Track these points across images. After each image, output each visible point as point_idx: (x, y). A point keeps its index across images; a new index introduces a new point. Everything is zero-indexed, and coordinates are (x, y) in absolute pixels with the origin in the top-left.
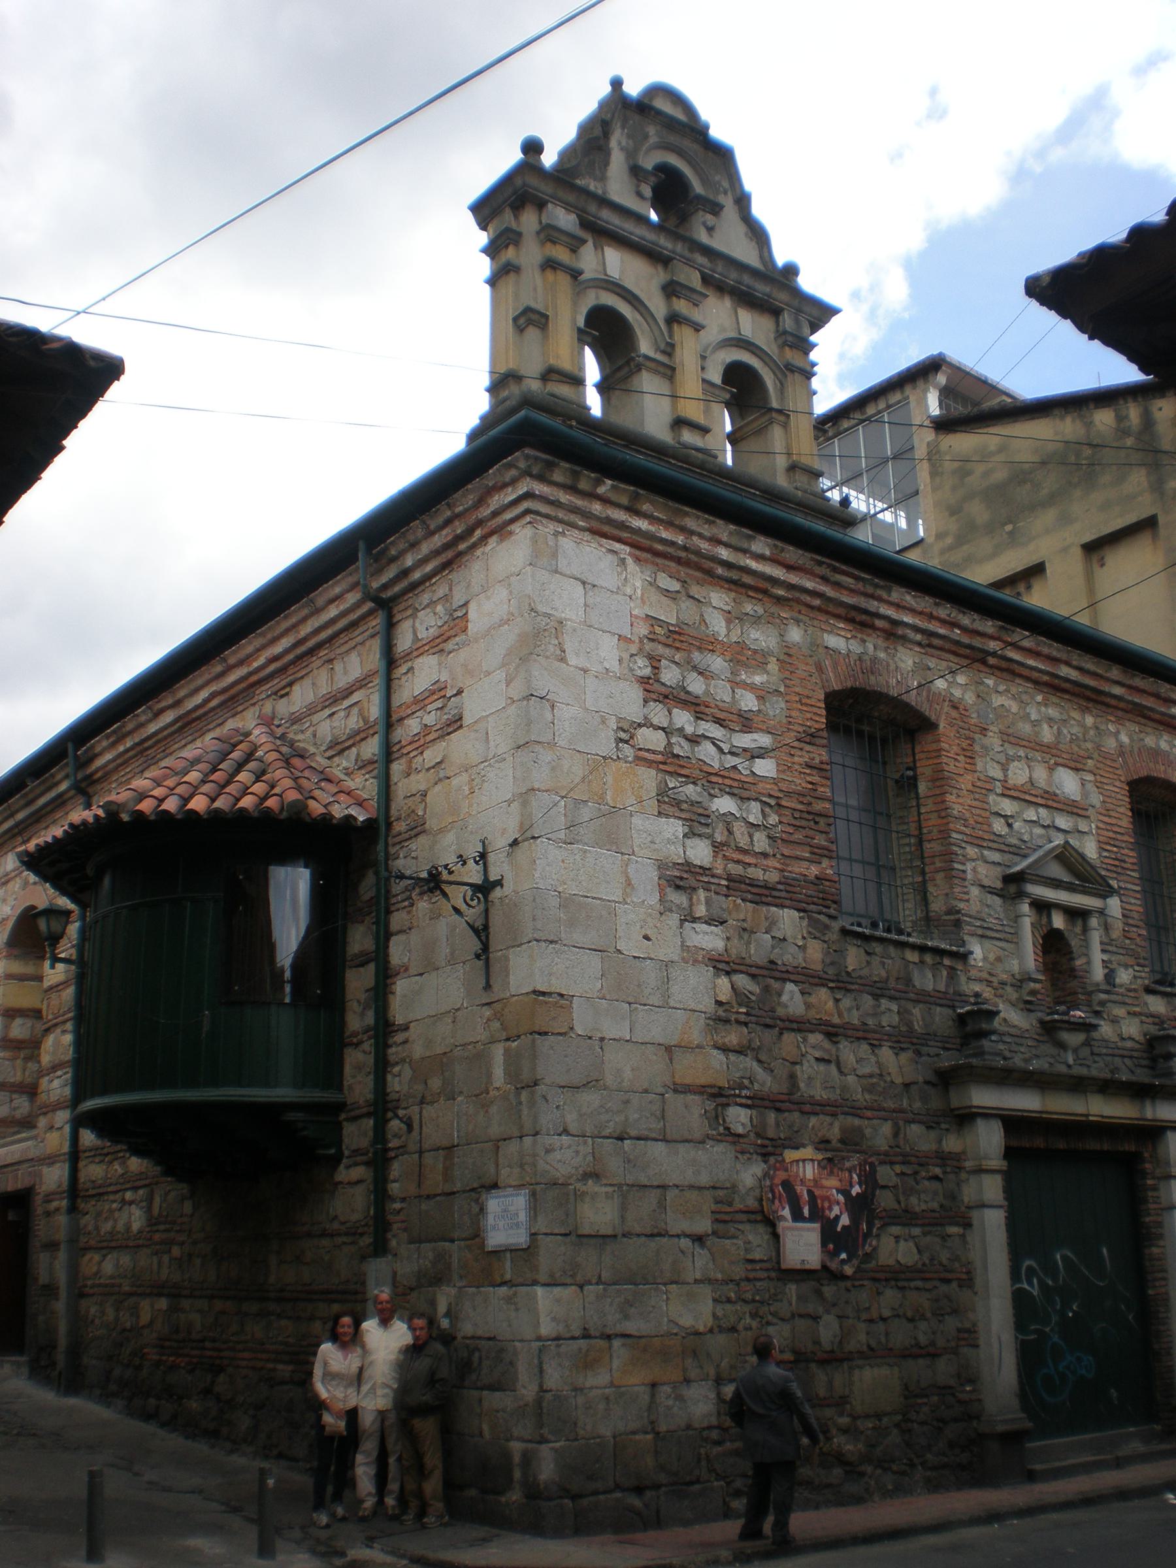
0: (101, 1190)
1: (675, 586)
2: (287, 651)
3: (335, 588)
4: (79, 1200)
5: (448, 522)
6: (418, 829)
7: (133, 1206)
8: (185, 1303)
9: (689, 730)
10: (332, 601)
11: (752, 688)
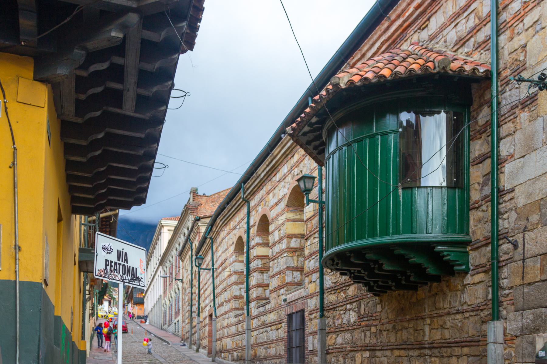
0: (335, 306)
4: (325, 312)
7: (351, 311)
8: (378, 353)
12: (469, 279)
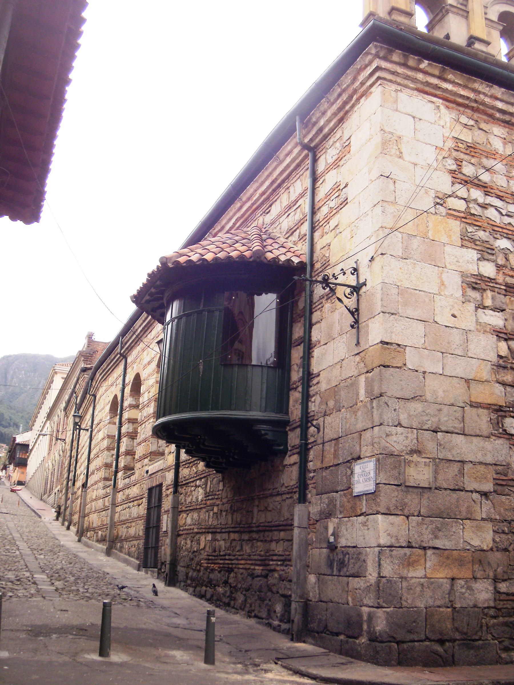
8: (218, 536)
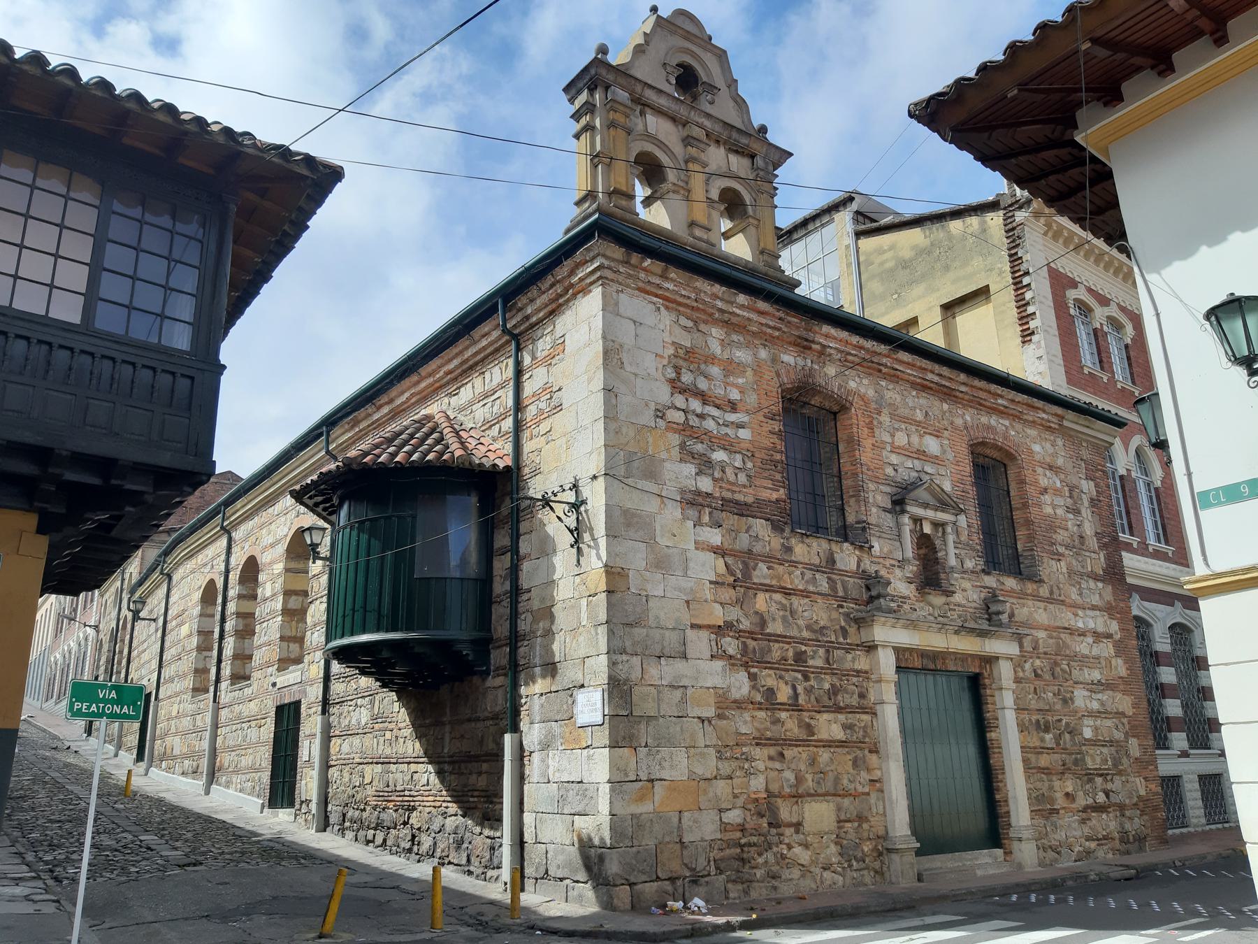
1: (690, 324)
2: (457, 367)
3: (485, 327)
5: (552, 286)
6: (536, 472)
9: (699, 411)
10: (483, 336)
11: (736, 386)
12: (492, 682)
